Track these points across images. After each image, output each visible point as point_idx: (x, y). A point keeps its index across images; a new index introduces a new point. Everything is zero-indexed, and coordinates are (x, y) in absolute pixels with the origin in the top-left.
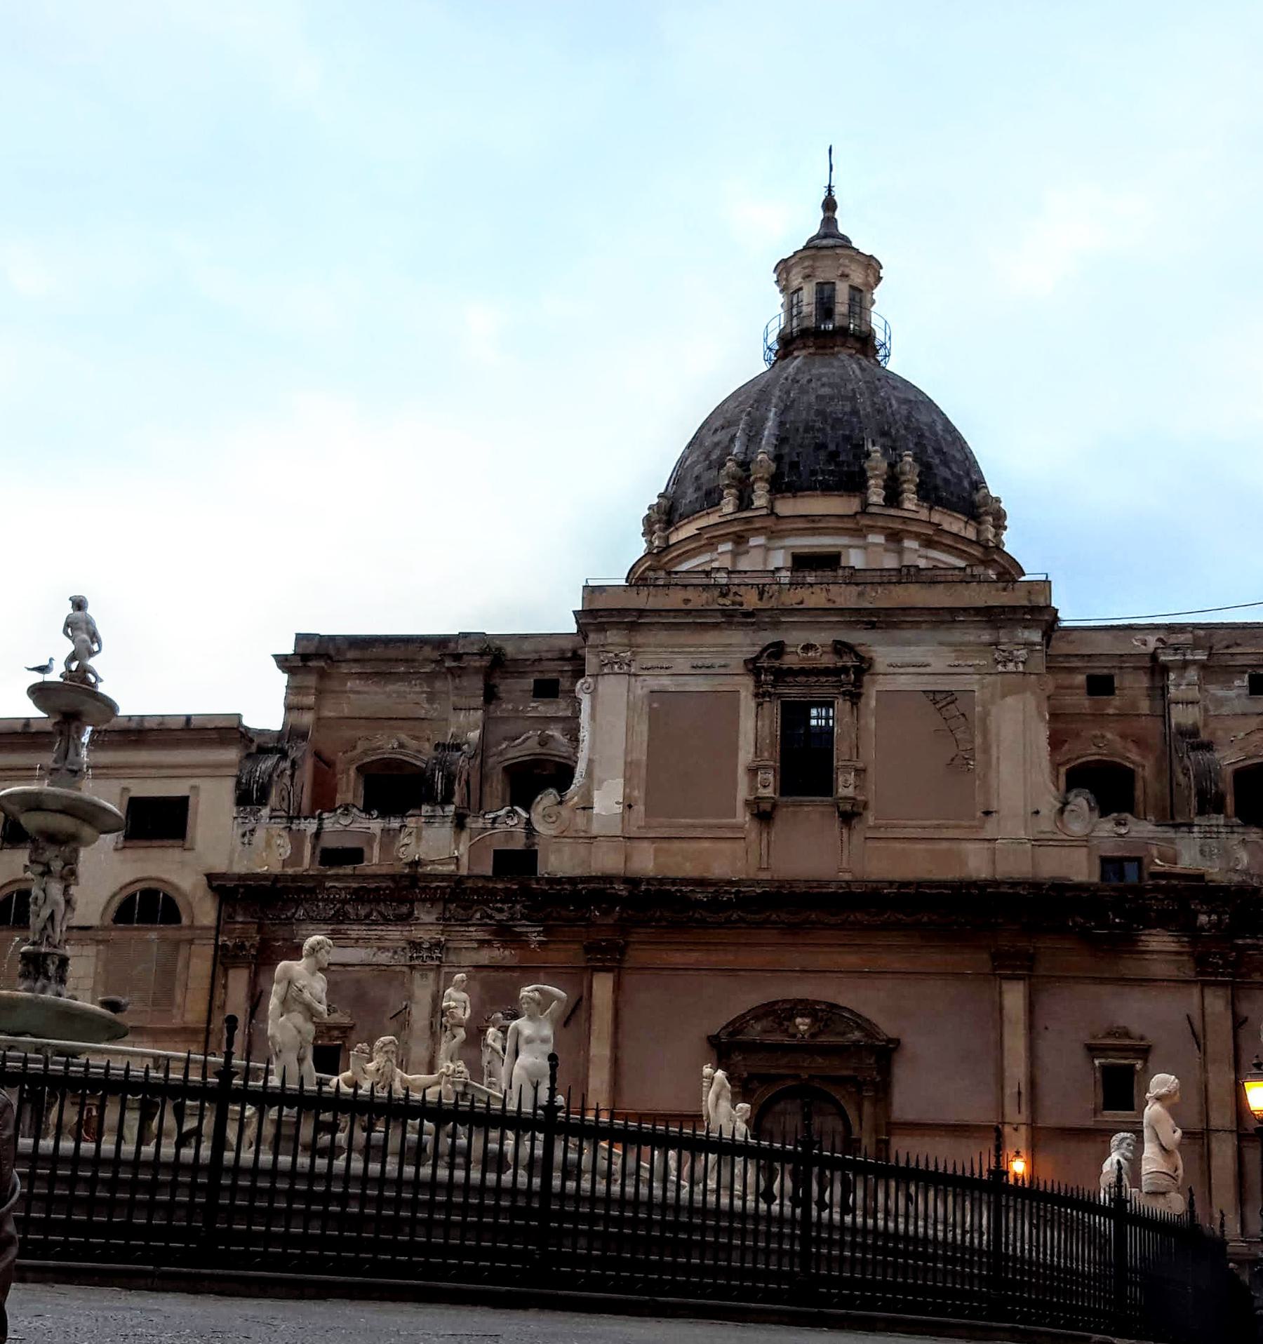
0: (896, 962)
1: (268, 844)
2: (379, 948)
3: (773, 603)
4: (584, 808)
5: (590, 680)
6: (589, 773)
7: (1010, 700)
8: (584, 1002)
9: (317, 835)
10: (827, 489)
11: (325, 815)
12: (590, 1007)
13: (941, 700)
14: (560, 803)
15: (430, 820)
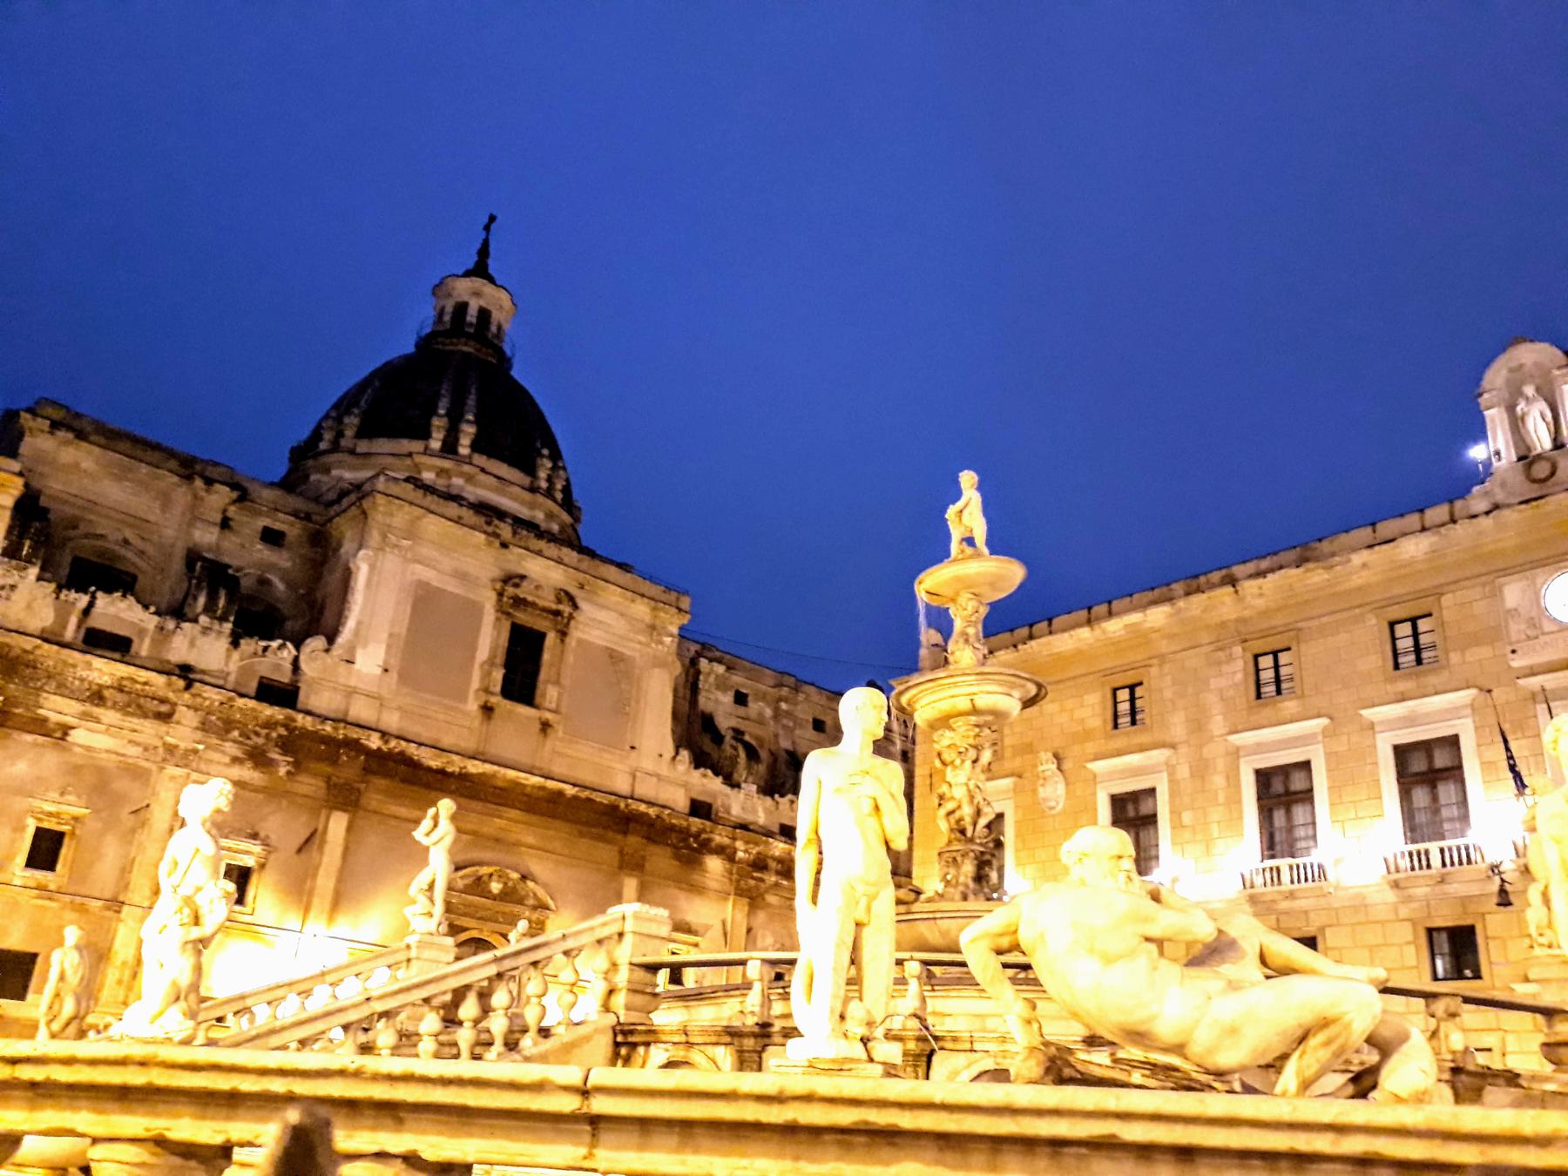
0: (557, 845)
1: (29, 606)
2: (130, 742)
3: (522, 544)
4: (348, 661)
5: (371, 553)
6: (357, 633)
7: (657, 670)
8: (318, 835)
9: (86, 612)
10: (512, 462)
11: (100, 594)
12: (323, 842)
13: (614, 657)
14: (327, 651)
15: (206, 631)
